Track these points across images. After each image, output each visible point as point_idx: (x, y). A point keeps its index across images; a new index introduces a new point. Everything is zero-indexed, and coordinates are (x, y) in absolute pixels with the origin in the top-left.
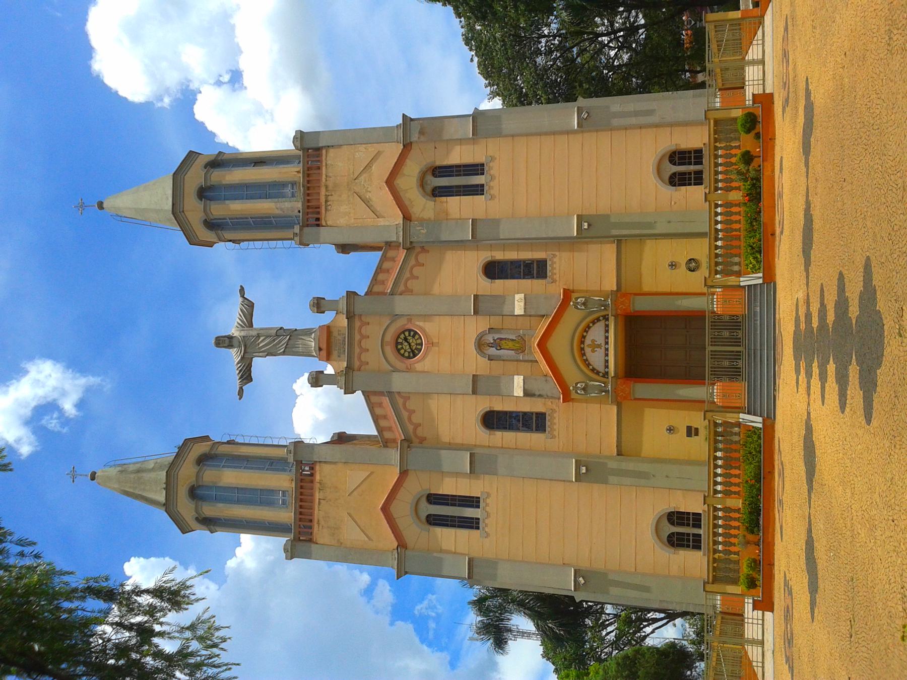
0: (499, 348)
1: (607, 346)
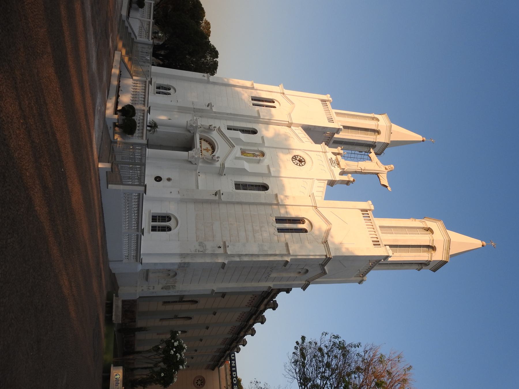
0: (254, 154)
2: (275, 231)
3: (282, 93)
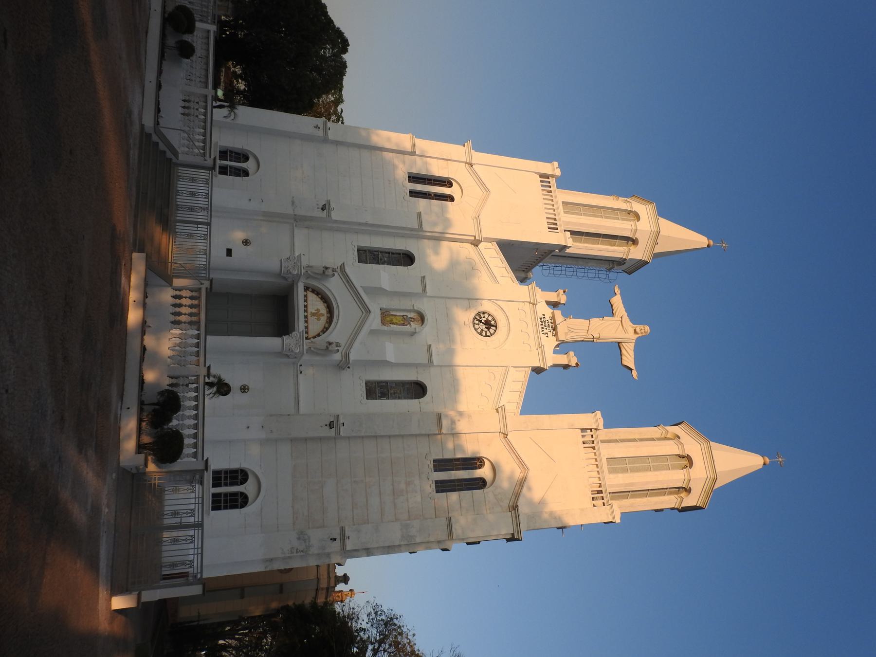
0: (405, 317)
1: (306, 314)
2: (430, 487)
3: (468, 164)
